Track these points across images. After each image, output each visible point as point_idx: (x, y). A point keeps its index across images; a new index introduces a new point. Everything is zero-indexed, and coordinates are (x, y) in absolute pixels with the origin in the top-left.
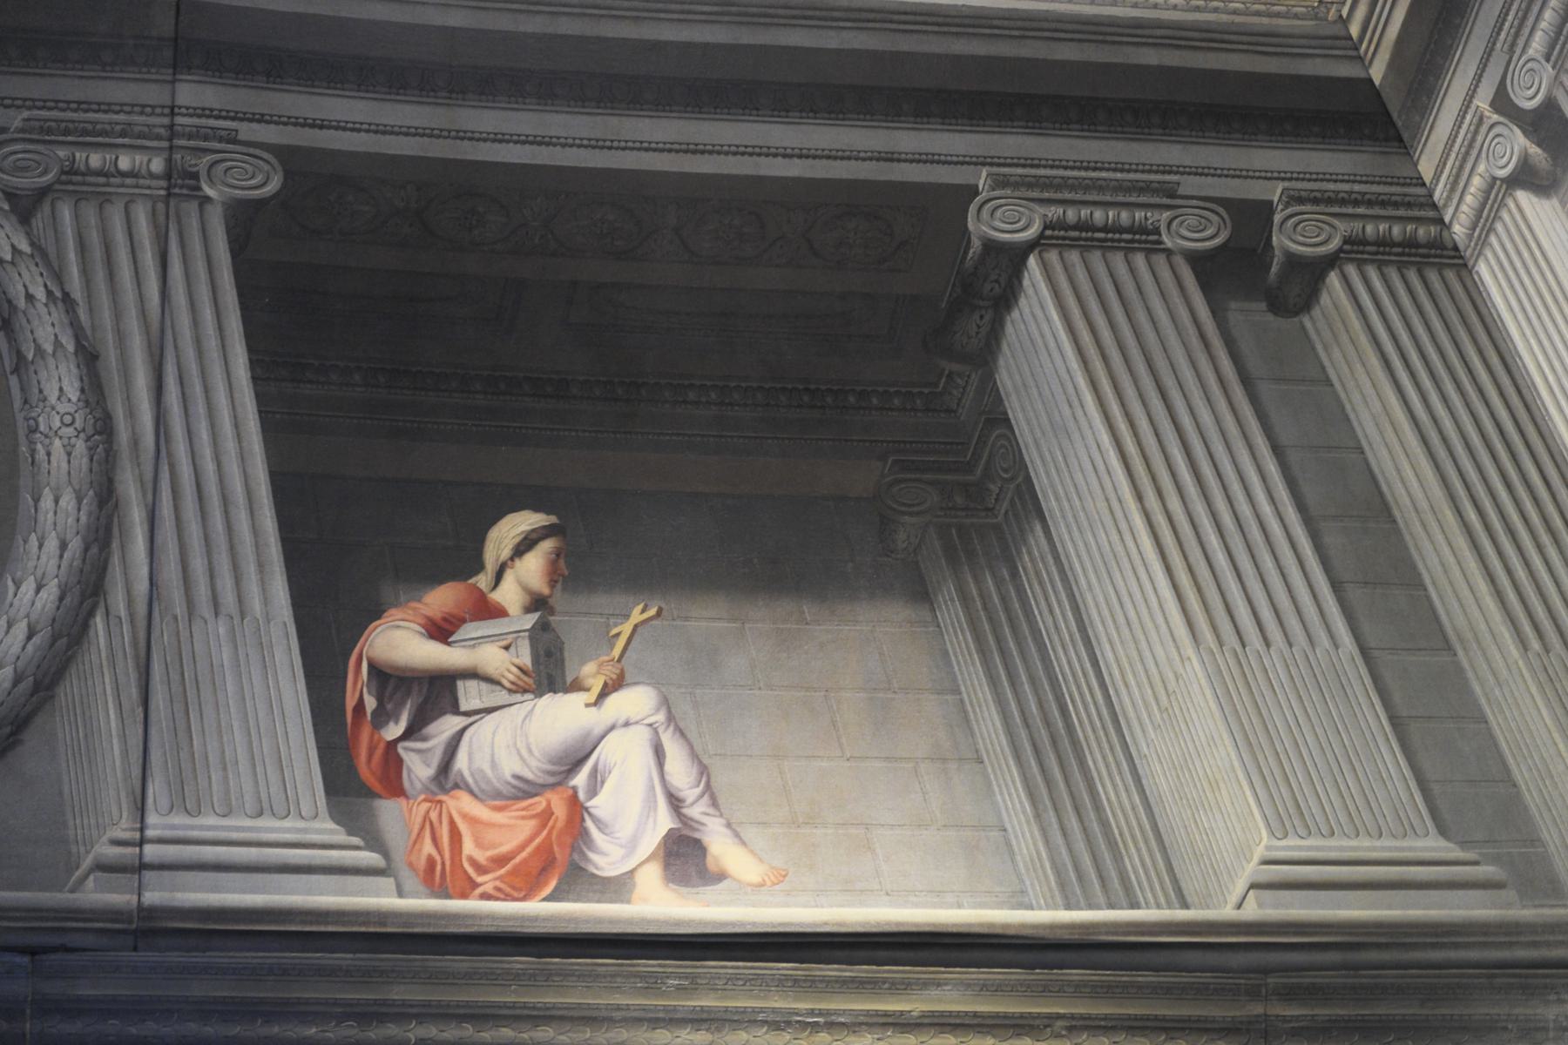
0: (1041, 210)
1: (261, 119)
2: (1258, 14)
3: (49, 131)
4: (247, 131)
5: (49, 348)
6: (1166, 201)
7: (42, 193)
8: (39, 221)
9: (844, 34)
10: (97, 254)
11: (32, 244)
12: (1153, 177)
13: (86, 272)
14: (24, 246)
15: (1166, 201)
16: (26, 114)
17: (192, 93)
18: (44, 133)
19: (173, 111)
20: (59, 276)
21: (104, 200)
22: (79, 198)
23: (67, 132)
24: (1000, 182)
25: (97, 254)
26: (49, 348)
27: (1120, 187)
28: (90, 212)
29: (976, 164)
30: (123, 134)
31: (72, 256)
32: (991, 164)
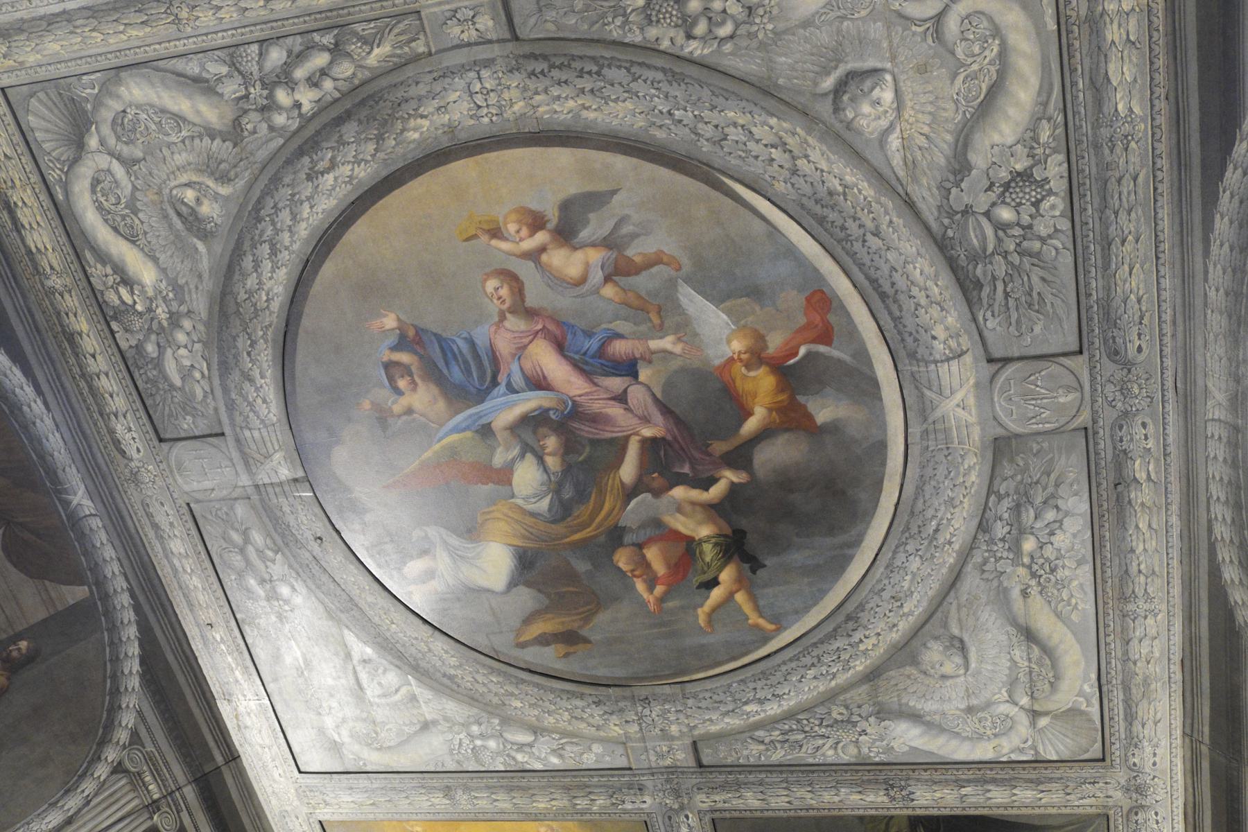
1: (190, 814)
3: (151, 760)
4: (185, 816)
5: (66, 808)
7: (126, 771)
8: (114, 777)
10: (112, 800)
11: (105, 780)
13: (103, 800)
14: (102, 779)
16: (154, 750)
17: (190, 792)
18: (149, 759)
19: (179, 789)
20: (96, 795)
21: (134, 789)
22: (131, 783)
23: (154, 765)
25: (112, 800)
26: (66, 808)
28: (128, 788)
30: (162, 780)
31: (106, 794)
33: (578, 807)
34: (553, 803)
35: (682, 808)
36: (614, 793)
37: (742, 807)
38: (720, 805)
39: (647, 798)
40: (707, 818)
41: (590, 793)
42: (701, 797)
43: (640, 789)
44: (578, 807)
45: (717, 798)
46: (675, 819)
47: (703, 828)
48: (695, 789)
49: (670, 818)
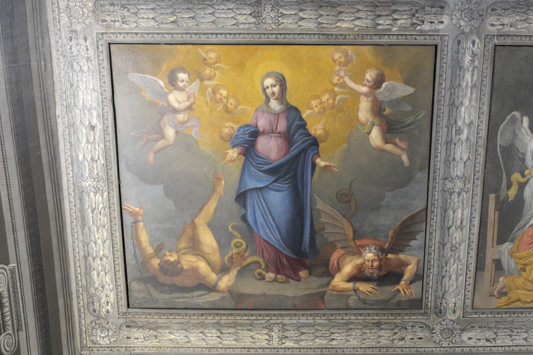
0: (5, 289)
2: (81, 330)
6: (16, 329)
9: (52, 201)
12: (23, 321)
15: (16, 329)
24: (12, 272)
27: (18, 312)
29: (17, 261)
32: (18, 266)
33: (380, 27)
34: (357, 23)
35: (471, 32)
36: (417, 11)
37: (525, 32)
38: (506, 29)
39: (445, 19)
40: (490, 46)
41: (395, 11)
42: (492, 19)
43: (442, 7)
44: (380, 27)
45: (506, 21)
46: (463, 44)
47: (484, 55)
48: (489, 11)
49: (459, 42)
